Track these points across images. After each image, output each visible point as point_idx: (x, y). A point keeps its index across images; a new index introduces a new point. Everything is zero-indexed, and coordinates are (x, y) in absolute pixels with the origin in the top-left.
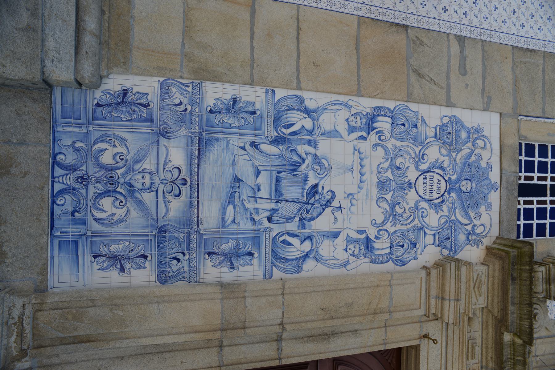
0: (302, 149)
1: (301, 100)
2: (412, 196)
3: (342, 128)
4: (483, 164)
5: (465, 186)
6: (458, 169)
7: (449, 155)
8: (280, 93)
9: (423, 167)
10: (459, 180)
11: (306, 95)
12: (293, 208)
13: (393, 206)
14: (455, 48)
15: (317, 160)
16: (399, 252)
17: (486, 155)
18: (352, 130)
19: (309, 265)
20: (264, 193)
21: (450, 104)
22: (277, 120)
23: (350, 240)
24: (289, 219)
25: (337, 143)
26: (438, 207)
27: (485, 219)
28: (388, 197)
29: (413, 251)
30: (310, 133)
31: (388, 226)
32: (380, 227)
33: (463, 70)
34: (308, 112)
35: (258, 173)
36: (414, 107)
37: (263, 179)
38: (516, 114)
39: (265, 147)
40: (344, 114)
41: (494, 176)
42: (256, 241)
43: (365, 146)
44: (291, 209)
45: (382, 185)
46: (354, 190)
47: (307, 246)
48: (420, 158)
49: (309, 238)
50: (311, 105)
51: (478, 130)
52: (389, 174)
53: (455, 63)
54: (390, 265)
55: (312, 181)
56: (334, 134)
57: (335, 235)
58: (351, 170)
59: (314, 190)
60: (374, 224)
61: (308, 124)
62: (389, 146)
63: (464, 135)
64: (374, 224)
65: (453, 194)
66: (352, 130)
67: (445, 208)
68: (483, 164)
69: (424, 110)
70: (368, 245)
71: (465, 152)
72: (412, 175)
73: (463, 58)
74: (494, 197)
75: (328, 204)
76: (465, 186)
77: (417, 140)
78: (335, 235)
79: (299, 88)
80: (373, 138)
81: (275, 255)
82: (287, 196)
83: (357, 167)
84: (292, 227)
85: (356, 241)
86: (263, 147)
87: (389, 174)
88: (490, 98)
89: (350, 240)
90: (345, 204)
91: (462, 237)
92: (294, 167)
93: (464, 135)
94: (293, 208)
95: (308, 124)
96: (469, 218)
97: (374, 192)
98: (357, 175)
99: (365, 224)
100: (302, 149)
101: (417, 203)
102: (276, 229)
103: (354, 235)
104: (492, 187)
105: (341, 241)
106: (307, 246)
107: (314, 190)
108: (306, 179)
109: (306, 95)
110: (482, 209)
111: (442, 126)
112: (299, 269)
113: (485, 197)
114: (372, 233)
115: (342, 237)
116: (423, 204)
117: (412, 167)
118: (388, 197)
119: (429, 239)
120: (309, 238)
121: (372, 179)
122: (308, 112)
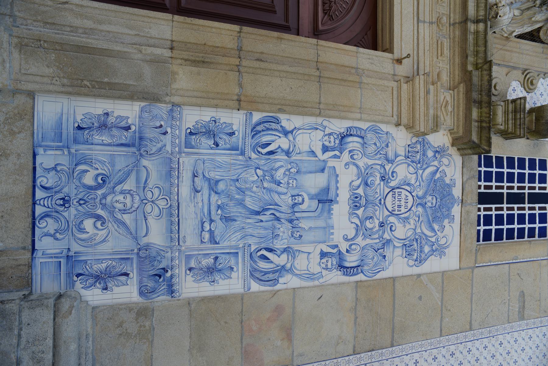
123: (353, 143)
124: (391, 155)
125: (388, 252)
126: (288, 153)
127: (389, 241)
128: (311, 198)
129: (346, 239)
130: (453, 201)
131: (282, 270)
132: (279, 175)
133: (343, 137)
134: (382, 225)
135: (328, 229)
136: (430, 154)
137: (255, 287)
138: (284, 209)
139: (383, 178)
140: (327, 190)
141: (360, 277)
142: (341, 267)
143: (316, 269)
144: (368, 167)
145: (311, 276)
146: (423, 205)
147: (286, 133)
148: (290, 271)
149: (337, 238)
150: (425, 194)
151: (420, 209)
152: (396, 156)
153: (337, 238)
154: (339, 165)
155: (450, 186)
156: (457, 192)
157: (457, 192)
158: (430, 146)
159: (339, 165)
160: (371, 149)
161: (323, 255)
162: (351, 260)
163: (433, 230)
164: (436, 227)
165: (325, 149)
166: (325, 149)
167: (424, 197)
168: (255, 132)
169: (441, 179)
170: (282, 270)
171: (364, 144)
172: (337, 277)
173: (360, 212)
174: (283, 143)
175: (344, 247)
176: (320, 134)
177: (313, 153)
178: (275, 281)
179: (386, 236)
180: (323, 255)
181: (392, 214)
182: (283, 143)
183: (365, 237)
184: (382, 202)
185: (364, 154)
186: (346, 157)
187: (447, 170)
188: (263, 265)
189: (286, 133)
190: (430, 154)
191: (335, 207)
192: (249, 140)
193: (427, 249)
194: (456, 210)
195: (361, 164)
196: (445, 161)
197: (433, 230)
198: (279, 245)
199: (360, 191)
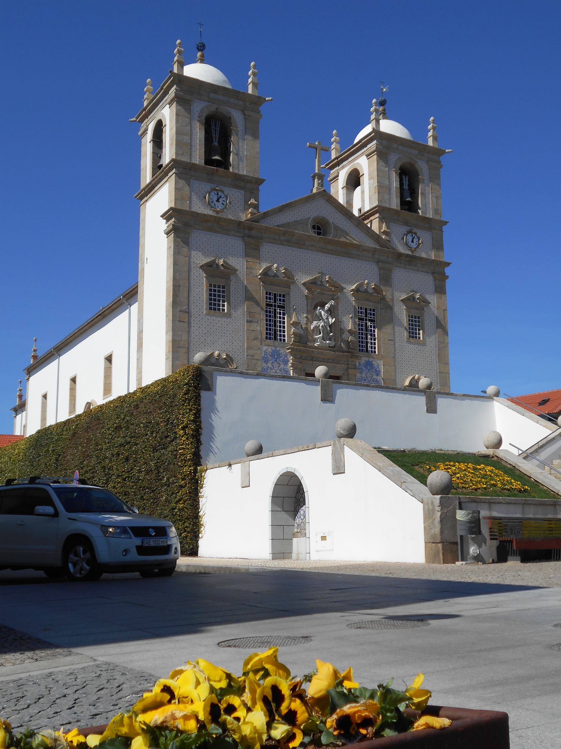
4: (271, 351)
5: (276, 357)
10: (275, 358)
29: (288, 372)
48: (271, 368)
63: (266, 356)
65: (277, 360)
68: (271, 351)
76: (276, 357)
77: (267, 369)
91: (286, 358)
93: (266, 356)
96: (282, 356)
101: (279, 370)
110: (280, 352)
113: (278, 351)
116: (279, 368)
119: (286, 367)
134: (373, 381)
136: (360, 367)
139: (365, 381)
146: (370, 370)
150: (368, 369)
152: (361, 376)
156: (367, 359)
157: (367, 359)
158: (359, 367)
190: (360, 367)
194: (371, 360)
196: (361, 362)
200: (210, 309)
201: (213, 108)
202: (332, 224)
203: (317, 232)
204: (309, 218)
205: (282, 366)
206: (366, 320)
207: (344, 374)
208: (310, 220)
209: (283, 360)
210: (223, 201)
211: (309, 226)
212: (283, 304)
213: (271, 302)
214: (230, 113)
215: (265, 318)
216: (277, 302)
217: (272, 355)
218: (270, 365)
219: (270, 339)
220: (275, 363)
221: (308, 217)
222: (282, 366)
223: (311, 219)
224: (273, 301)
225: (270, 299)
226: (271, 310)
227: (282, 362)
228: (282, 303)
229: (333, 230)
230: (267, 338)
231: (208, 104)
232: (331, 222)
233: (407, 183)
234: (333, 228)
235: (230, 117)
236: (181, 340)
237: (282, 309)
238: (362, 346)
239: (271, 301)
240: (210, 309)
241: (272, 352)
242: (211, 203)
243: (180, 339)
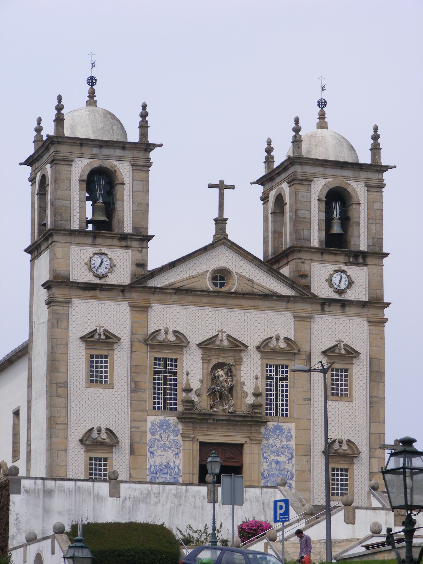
0: (158, 468)
1: (149, 468)
2: (167, 443)
3: (153, 460)
4: (159, 422)
6: (161, 429)
7: (157, 432)
8: (148, 473)
9: (160, 440)
10: (163, 429)
11: (147, 468)
12: (169, 471)
13: (169, 448)
14: (133, 430)
15: (160, 466)
16: (178, 446)
17: (158, 421)
18: (153, 458)
19: (180, 468)
20: (166, 476)
21: (146, 432)
22: (153, 473)
23: (175, 459)
24: (171, 471)
25: (156, 461)
26: (169, 436)
27: (172, 421)
28: (167, 449)
30: (155, 467)
31: (173, 449)
32: (173, 451)
33: (138, 428)
34: (151, 467)
35: (162, 478)
36: (148, 442)
37: (164, 477)
38: (147, 411)
39: (158, 476)
40: (150, 459)
41: (162, 418)
42: (175, 478)
43: (157, 455)
44: (169, 471)
45: (165, 450)
46: (165, 457)
47: (176, 468)
49: (175, 467)
50: (149, 467)
51: (152, 423)
52: (162, 449)
53: (137, 430)
54: (181, 449)
55: (164, 467)
56: (154, 461)
57: (174, 462)
58: (161, 458)
59: (166, 466)
60: (172, 453)
61: (153, 467)
62: (156, 448)
63: (153, 428)
64: (172, 453)
65: (167, 431)
66: (153, 458)
67: (170, 434)
68: (159, 422)
69: (148, 439)
70: (177, 454)
71: (157, 427)
72: (162, 443)
73: (135, 427)
74: (167, 418)
75: (168, 463)
76: (165, 427)
77: (155, 441)
78: (174, 462)
79: (146, 469)
80: (155, 452)
81: (178, 474)
82: (166, 472)
83: (161, 456)
84: (172, 471)
85: (176, 457)
86: (158, 476)
87: (162, 449)
88: (144, 419)
89: (175, 459)
90: (168, 459)
91: (176, 429)
92: (161, 470)
93: (153, 428)
94: (169, 471)
95: (153, 467)
97: (166, 452)
98: (162, 457)
99: (172, 455)
100: (158, 468)
102: (173, 474)
103: (174, 457)
104: (165, 419)
105: (175, 460)
106: (176, 468)
107: (166, 466)
108: (163, 468)
109: (147, 468)
110: (170, 422)
111: (152, 434)
112: (180, 470)
113: (167, 421)
114: (174, 453)
115: (175, 460)
116: (169, 439)
117: (161, 442)
118: (167, 449)
119: (176, 438)
120: (175, 467)
121: (163, 453)
122: (151, 467)
123: (265, 455)
124: (267, 445)
125: (289, 446)
126: (268, 471)
127: (287, 446)
128: (277, 466)
129: (285, 458)
130: (278, 425)
131: (291, 473)
132: (272, 473)
133: (265, 458)
134: (283, 448)
135: (283, 462)
136: (267, 433)
137: (294, 479)
138: (279, 472)
139: (273, 447)
140: (275, 462)
141: (294, 455)
142: (291, 459)
143: (291, 465)
144: (270, 452)
145: (293, 466)
146: (279, 435)
147: (264, 471)
148: (291, 471)
149: (285, 460)
151: (280, 436)
153: (285, 460)
154: (270, 459)
155: (274, 426)
156: (275, 424)
158: (265, 433)
159: (270, 459)
160: (266, 451)
161: (288, 463)
162: (290, 456)
163: (284, 432)
164: (284, 431)
165: (267, 462)
166: (267, 462)
167: (276, 435)
168: (264, 478)
169: (272, 429)
170: (291, 473)
171: (266, 453)
172: (293, 461)
173: (280, 454)
174: (266, 472)
175: (287, 458)
176: (264, 464)
177: (268, 465)
178: (293, 474)
179: (285, 447)
180: (288, 463)
181: (280, 445)
182: (266, 472)
183: (285, 453)
184: (278, 448)
185: (268, 452)
186: (268, 457)
187: (270, 427)
188: (290, 477)
189: (264, 471)
190: (267, 433)
191: (279, 460)
192: (266, 479)
193: (289, 434)
194: (280, 424)
195: (270, 453)
197: (284, 432)
198: (286, 474)
199: (275, 454)
200: (92, 381)
201: (96, 164)
202: (235, 274)
203: (220, 283)
204: (207, 271)
205: (172, 437)
206: (277, 379)
207: (246, 442)
208: (208, 273)
209: (174, 430)
210: (107, 265)
211: (207, 280)
212: (174, 369)
213: (160, 368)
214: (115, 166)
215: (152, 386)
216: (167, 367)
217: (161, 426)
218: (157, 437)
219: (159, 408)
220: (164, 434)
221: (205, 270)
222: (172, 437)
223: (210, 271)
224: (163, 367)
225: (159, 365)
226: (161, 377)
227: (172, 432)
228: (173, 368)
229: (236, 281)
230: (154, 408)
231: (91, 160)
232: (234, 272)
233: (338, 210)
234: (236, 278)
235: (115, 171)
236: (60, 417)
237: (173, 375)
238: (271, 409)
239: (161, 367)
240: (92, 381)
241: (160, 423)
242: (93, 269)
243: (59, 416)
